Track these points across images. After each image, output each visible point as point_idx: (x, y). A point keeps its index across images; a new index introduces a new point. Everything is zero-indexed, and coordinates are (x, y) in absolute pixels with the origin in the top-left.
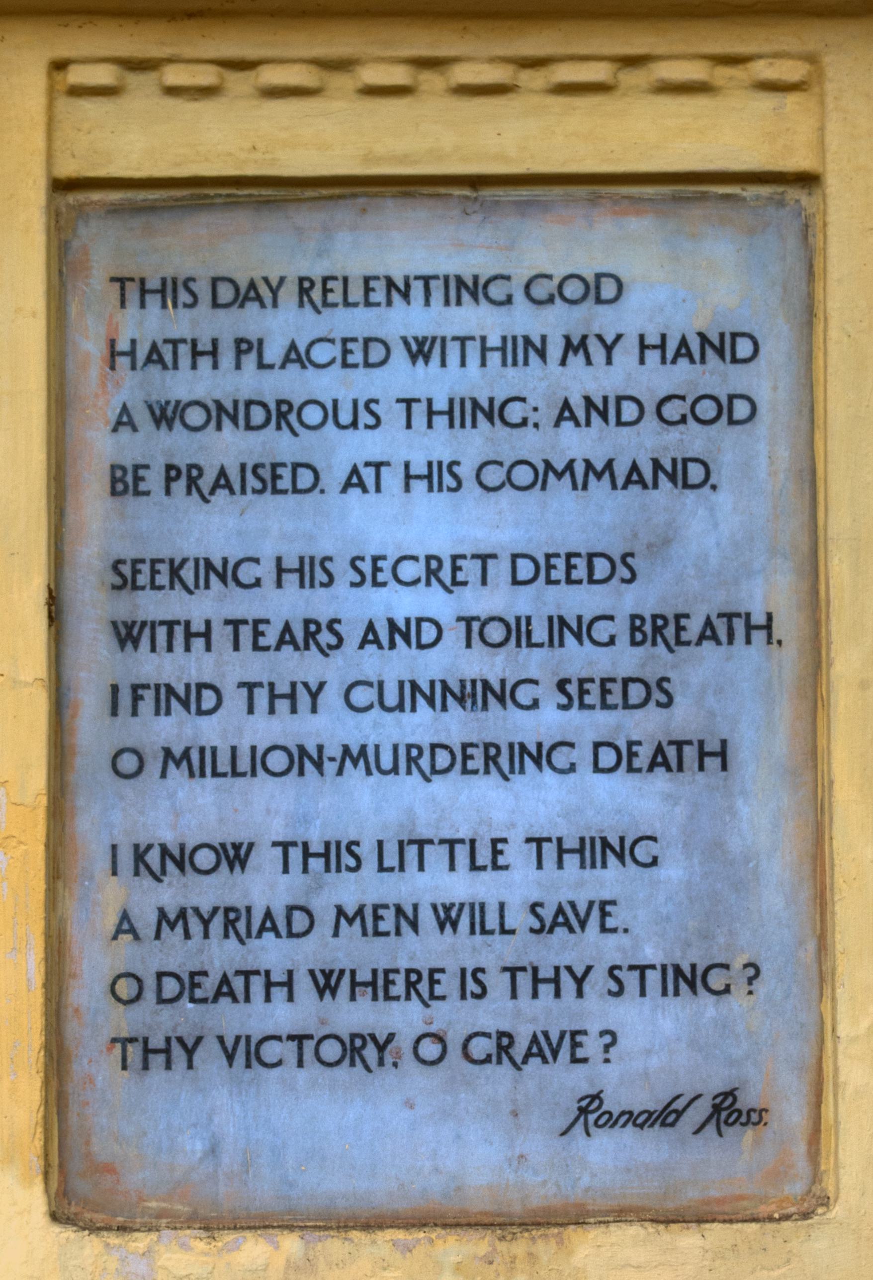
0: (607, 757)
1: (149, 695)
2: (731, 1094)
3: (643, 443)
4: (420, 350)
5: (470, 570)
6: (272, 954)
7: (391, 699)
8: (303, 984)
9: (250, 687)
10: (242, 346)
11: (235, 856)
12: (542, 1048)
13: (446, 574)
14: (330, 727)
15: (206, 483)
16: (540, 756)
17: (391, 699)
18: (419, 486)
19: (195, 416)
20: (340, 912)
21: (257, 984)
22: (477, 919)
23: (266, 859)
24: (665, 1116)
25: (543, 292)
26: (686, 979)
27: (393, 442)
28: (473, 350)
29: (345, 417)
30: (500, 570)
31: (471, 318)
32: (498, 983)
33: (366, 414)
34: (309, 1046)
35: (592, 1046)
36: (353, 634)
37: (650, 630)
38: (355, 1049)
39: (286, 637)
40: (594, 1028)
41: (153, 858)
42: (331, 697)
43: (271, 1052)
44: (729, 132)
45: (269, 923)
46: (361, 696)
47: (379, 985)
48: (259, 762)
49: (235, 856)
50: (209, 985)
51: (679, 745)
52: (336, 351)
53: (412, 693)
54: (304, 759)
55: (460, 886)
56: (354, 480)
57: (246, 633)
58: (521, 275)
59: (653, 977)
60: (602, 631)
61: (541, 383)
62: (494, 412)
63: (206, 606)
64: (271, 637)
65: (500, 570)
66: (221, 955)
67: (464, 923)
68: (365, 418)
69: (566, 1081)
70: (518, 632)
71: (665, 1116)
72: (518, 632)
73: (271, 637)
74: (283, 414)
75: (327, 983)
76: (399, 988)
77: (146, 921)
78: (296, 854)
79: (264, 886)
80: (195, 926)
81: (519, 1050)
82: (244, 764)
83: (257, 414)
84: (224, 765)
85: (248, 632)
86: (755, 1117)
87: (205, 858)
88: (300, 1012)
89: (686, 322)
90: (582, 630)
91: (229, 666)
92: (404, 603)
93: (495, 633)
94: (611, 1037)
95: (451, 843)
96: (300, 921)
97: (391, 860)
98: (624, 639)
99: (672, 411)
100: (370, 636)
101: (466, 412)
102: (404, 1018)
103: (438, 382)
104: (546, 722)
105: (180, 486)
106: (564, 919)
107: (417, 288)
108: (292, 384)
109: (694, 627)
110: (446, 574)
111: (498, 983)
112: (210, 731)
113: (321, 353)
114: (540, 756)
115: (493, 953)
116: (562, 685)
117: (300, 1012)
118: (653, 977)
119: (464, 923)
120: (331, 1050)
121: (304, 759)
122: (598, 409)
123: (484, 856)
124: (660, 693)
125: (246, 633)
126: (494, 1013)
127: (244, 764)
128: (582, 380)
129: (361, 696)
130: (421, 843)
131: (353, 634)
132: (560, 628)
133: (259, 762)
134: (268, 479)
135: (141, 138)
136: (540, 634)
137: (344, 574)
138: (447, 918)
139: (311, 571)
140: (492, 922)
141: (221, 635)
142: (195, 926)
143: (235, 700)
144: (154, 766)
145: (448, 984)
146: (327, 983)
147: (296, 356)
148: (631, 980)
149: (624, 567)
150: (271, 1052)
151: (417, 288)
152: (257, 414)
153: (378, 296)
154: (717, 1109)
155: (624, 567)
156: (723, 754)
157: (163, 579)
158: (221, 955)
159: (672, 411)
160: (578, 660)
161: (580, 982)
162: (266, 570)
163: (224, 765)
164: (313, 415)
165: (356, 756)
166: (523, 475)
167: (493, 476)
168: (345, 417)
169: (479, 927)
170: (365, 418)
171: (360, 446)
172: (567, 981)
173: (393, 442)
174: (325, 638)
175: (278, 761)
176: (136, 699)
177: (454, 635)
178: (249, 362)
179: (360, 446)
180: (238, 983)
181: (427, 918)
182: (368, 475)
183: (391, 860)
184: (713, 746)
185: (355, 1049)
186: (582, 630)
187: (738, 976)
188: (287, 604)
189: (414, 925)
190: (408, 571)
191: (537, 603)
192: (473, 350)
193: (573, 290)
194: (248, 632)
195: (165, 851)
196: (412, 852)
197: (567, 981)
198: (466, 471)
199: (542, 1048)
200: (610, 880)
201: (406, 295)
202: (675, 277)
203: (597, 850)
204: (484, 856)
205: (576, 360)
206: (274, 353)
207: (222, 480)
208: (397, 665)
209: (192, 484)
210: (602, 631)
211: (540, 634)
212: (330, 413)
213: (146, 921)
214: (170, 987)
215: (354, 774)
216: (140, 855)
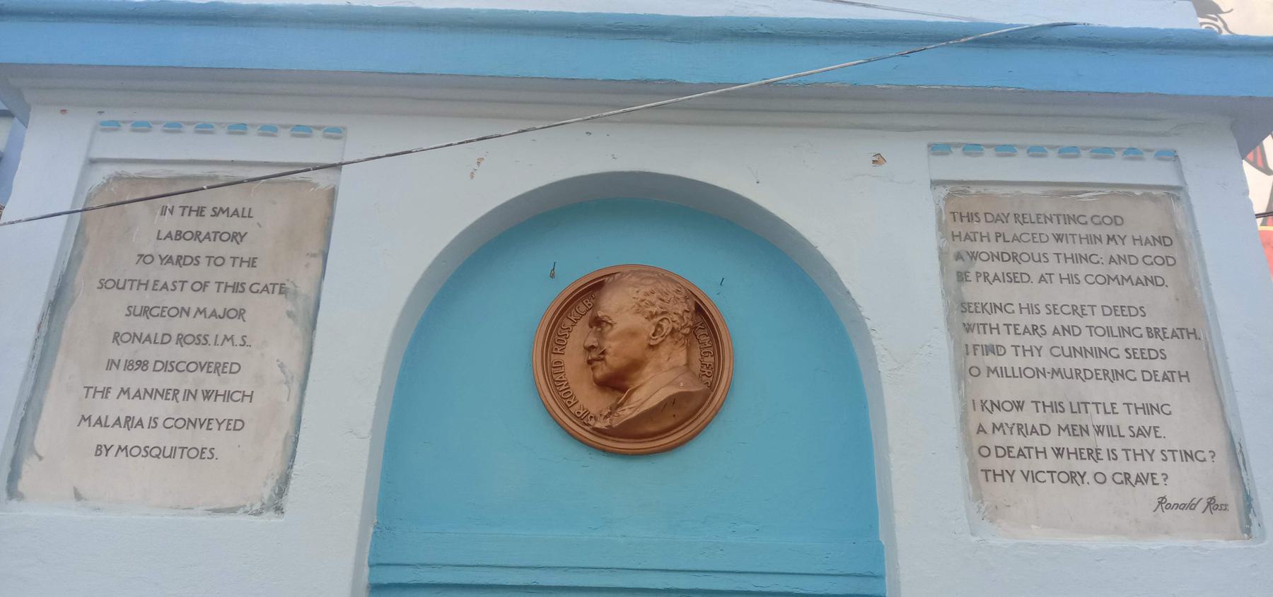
0: (1147, 376)
1: (979, 349)
2: (1213, 498)
3: (1140, 271)
4: (1059, 238)
5: (1088, 310)
6: (1036, 441)
7: (1067, 353)
8: (1050, 453)
9: (1016, 347)
10: (998, 235)
11: (1019, 406)
12: (1141, 479)
13: (1079, 311)
14: (1045, 362)
15: (991, 278)
16: (1123, 375)
17: (1067, 353)
18: (1065, 282)
19: (984, 256)
20: (1060, 427)
21: (1033, 452)
22: (1111, 431)
23: (1029, 407)
24: (1191, 506)
25: (1098, 221)
26: (1189, 456)
27: (1053, 266)
28: (1077, 238)
29: (1036, 258)
30: (1098, 310)
31: (1073, 228)
32: (1121, 455)
33: (1043, 258)
34: (1055, 475)
35: (1159, 479)
36: (1050, 330)
37: (1153, 333)
38: (1072, 477)
39: (1026, 330)
40: (1159, 472)
41: (988, 405)
42: (1045, 352)
43: (1040, 476)
44: (1154, 173)
45: (1034, 430)
46: (1056, 351)
47: (1078, 453)
48: (1022, 373)
49: (1019, 406)
50: (1015, 452)
51: (1172, 372)
52: (1030, 237)
53: (1074, 352)
54: (1038, 373)
55: (1101, 419)
56: (1042, 279)
57: (1011, 328)
58: (1089, 215)
59: (1177, 455)
60: (1137, 332)
61: (1103, 250)
62: (1087, 259)
63: (997, 319)
64: (1021, 330)
65: (1098, 310)
66: (1018, 441)
67: (1106, 432)
68: (1043, 259)
69: (1151, 493)
70: (1108, 332)
71: (1191, 506)
72: (1108, 332)
73: (1021, 330)
74: (1014, 257)
75: (1059, 452)
76: (1085, 455)
77: (989, 428)
78: (1040, 405)
79: (1029, 417)
80: (1007, 431)
81: (1133, 479)
82: (1017, 373)
83: (1006, 257)
84: (1010, 373)
85: (1013, 328)
86: (1224, 507)
87: (1007, 406)
88: (1051, 463)
89: (1148, 233)
90: (1130, 332)
91: (1007, 340)
92: (1067, 321)
93: (1100, 331)
94: (1166, 477)
95: (1097, 404)
96: (1045, 430)
97: (1075, 409)
98: (1145, 334)
99: (1148, 260)
100: (1056, 331)
101: (1078, 258)
102: (1088, 466)
103: (1067, 248)
104: (1122, 364)
105: (982, 279)
106: (1141, 432)
107: (1055, 218)
108: (1017, 248)
109: (1169, 334)
110: (1079, 311)
111: (1121, 455)
112: (1001, 362)
113: (1024, 237)
114: (1119, 375)
115: (1116, 444)
116: (1126, 350)
117: (1051, 463)
118: (1177, 455)
119: (1106, 432)
120: (1064, 477)
121: (1038, 373)
122: (1122, 259)
123: (1109, 409)
124: (1161, 354)
125: (1011, 328)
126: (1122, 465)
127: (1017, 373)
128: (1116, 250)
129: (1056, 351)
130: (1086, 403)
131: (1050, 330)
132: (1124, 332)
133: (1022, 373)
134: (1013, 278)
135: (960, 167)
136: (1116, 333)
137: (1044, 311)
138: (1099, 431)
139: (1032, 309)
140: (1116, 433)
141: (1003, 329)
142: (1007, 431)
143: (1011, 351)
144: (984, 372)
145: (1103, 455)
146: (1059, 452)
147: (1016, 239)
148: (1169, 455)
149: (1141, 311)
150: (1040, 476)
151: (1055, 218)
152: (1006, 257)
153: (1042, 220)
154: (1209, 504)
155: (1141, 311)
156: (1187, 376)
157: (979, 309)
158: (1018, 441)
159: (1148, 260)
160: (1131, 342)
161: (1151, 455)
162: (1016, 308)
163: (1010, 373)
164: (1025, 257)
165: (1056, 372)
166: (1101, 280)
167: (1090, 279)
168: (1036, 258)
169: (1111, 434)
170: (1043, 259)
171: (1044, 268)
172: (1146, 455)
173: (1053, 266)
174: (1039, 331)
175: (1029, 373)
176: (975, 350)
177: (1086, 331)
178: (1001, 239)
179: (1044, 268)
180: (1026, 451)
181: (1091, 430)
182: (1047, 277)
183: (1075, 409)
184: (1183, 373)
185: (1072, 477)
186: (1130, 332)
187: (1208, 456)
188: (1026, 320)
189: (1087, 432)
190: (1066, 309)
191: (1117, 322)
192: (1077, 238)
193: (1107, 220)
194: (1013, 328)
195: (992, 403)
196: (1082, 407)
197: (1146, 455)
198: (1081, 278)
199: (1141, 479)
200: (1155, 419)
201: (1051, 220)
202: (1145, 219)
203: (1149, 409)
204: (1109, 409)
205: (1112, 243)
206: (1009, 238)
207: (996, 277)
208: (1067, 341)
209: (986, 278)
210: (1137, 332)
211: (1116, 333)
212: (1031, 257)
213: (989, 428)
214: (1001, 452)
215: (1058, 379)
216: (983, 404)
